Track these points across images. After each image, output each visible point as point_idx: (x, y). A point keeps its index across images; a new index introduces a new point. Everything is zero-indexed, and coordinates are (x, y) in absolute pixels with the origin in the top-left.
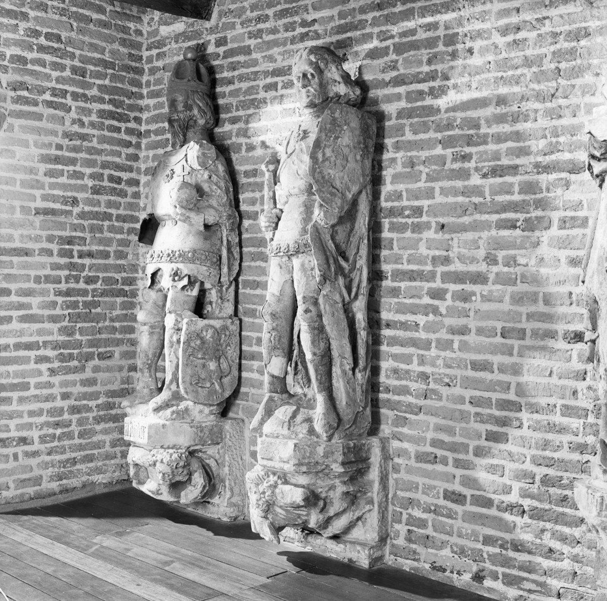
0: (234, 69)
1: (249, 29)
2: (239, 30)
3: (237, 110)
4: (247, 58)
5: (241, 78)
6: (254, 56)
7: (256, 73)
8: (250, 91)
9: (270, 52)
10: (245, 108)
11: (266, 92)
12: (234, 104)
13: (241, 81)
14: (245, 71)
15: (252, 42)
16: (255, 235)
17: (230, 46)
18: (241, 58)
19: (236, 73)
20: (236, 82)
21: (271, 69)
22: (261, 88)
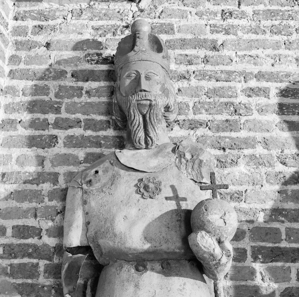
0: (190, 63)
1: (211, 22)
2: (193, 20)
3: (196, 111)
4: (210, 53)
5: (202, 75)
6: (226, 52)
7: (229, 73)
8: (215, 92)
9: (254, 52)
10: (212, 112)
11: (249, 96)
12: (191, 105)
13: (203, 79)
14: (209, 67)
15: (220, 38)
16: (243, 283)
17: (178, 36)
18: (202, 53)
19: (192, 68)
20: (192, 78)
21: (256, 72)
22: (239, 91)
